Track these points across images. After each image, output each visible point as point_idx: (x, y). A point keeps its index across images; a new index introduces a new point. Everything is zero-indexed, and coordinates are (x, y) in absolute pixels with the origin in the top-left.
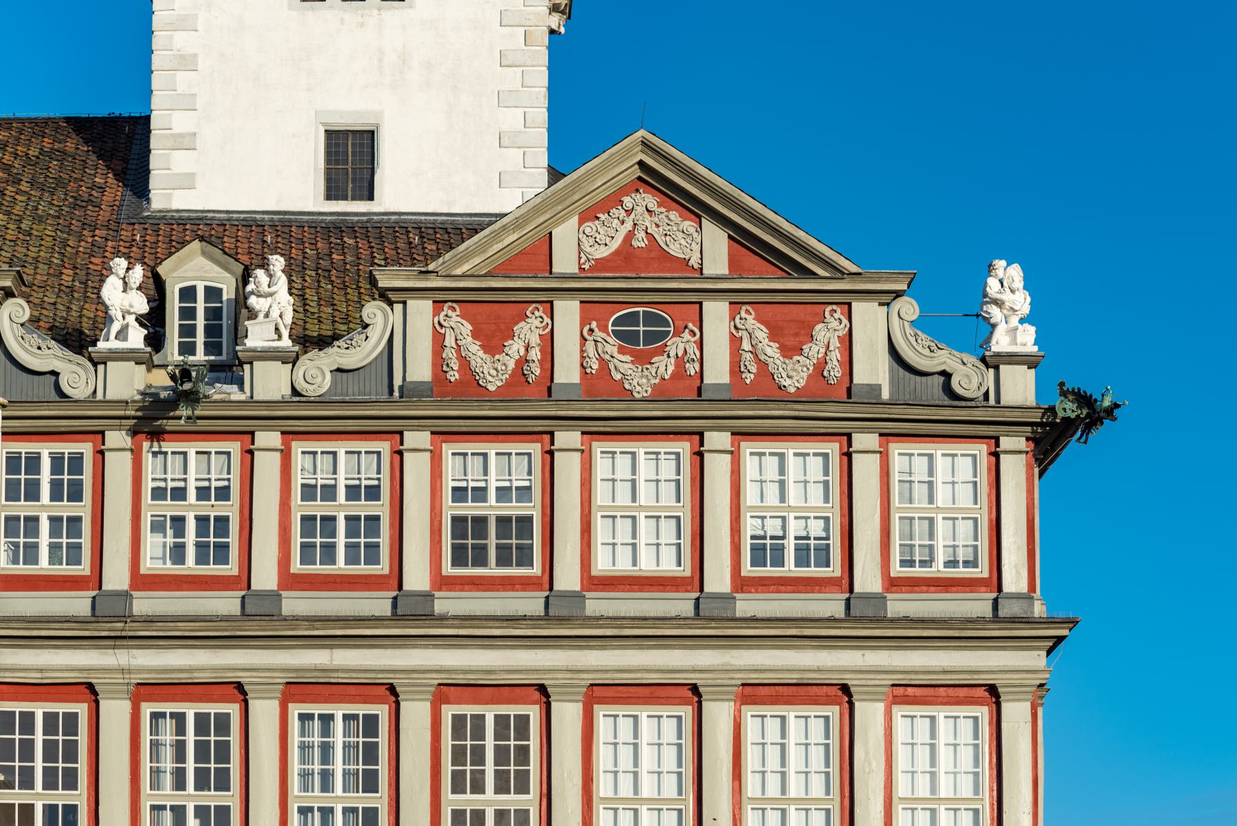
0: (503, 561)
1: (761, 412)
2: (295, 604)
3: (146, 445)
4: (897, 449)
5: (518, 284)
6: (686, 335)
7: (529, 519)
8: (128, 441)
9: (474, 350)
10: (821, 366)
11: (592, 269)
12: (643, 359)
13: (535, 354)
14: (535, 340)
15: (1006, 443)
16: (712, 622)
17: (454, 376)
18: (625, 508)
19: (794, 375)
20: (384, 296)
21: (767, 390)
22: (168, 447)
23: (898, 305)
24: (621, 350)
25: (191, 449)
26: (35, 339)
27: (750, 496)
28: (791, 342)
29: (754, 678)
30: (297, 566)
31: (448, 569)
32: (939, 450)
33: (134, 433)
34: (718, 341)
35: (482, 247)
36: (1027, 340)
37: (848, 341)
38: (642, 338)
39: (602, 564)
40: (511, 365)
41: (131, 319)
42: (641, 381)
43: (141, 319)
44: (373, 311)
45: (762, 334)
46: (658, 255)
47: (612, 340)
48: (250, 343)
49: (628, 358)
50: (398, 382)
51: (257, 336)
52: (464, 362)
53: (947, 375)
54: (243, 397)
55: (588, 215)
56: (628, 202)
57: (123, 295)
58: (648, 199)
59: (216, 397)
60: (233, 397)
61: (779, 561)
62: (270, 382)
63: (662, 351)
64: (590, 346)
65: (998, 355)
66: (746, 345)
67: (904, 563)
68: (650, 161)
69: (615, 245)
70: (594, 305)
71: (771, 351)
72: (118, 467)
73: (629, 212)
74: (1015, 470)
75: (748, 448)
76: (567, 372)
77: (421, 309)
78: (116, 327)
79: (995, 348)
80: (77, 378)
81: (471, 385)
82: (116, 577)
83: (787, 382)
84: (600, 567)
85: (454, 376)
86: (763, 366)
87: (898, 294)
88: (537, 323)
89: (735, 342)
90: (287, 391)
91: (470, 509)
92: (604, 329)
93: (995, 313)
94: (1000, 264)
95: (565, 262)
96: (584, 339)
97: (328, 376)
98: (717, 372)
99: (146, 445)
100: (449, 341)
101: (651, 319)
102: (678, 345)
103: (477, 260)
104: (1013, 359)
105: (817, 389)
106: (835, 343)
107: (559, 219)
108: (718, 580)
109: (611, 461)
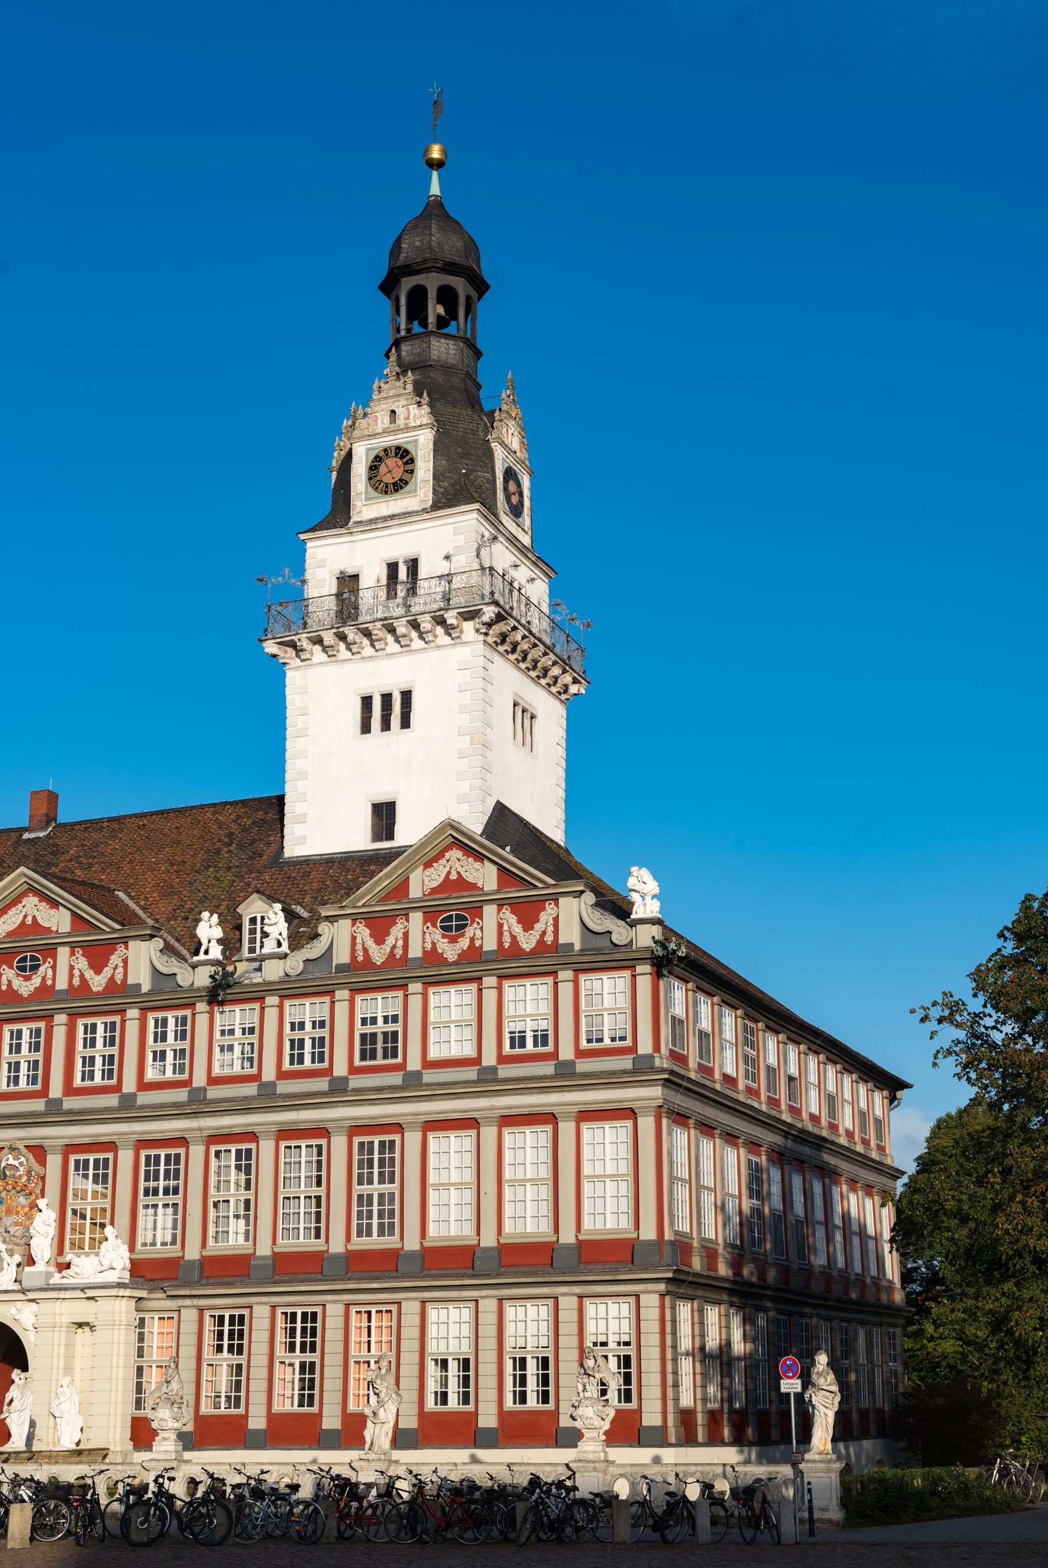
0: (385, 1057)
1: (513, 963)
2: (284, 1087)
3: (216, 1008)
4: (582, 977)
5: (388, 908)
6: (475, 925)
7: (397, 1032)
8: (207, 1008)
11: (429, 894)
12: (453, 940)
13: (400, 943)
14: (400, 935)
15: (640, 969)
16: (488, 1081)
17: (360, 959)
18: (449, 1023)
19: (528, 942)
20: (329, 919)
21: (515, 951)
22: (227, 1008)
23: (583, 896)
24: (444, 936)
25: (237, 1008)
26: (165, 958)
27: (509, 1010)
29: (506, 1112)
30: (286, 1065)
31: (357, 1062)
32: (605, 976)
33: (210, 1003)
35: (370, 890)
37: (556, 920)
38: (453, 928)
39: (434, 1054)
40: (388, 950)
41: (214, 942)
42: (450, 952)
43: (220, 941)
45: (513, 919)
46: (461, 884)
49: (446, 940)
51: (270, 947)
52: (365, 950)
54: (260, 980)
55: (428, 865)
56: (447, 855)
57: (209, 929)
58: (455, 854)
59: (246, 982)
60: (254, 981)
61: (523, 1044)
62: (273, 971)
63: (462, 935)
64: (427, 936)
65: (634, 920)
66: (505, 928)
67: (589, 1041)
72: (202, 1020)
73: (448, 861)
74: (644, 984)
75: (506, 984)
77: (347, 923)
80: (185, 977)
82: (199, 1080)
83: (524, 946)
84: (432, 1055)
85: (360, 959)
87: (582, 892)
88: (401, 926)
89: (500, 926)
90: (282, 974)
91: (369, 1029)
92: (434, 925)
95: (415, 891)
96: (424, 933)
97: (301, 965)
99: (216, 1008)
100: (359, 941)
101: (460, 917)
102: (469, 932)
103: (369, 897)
108: (489, 1059)
109: (437, 997)
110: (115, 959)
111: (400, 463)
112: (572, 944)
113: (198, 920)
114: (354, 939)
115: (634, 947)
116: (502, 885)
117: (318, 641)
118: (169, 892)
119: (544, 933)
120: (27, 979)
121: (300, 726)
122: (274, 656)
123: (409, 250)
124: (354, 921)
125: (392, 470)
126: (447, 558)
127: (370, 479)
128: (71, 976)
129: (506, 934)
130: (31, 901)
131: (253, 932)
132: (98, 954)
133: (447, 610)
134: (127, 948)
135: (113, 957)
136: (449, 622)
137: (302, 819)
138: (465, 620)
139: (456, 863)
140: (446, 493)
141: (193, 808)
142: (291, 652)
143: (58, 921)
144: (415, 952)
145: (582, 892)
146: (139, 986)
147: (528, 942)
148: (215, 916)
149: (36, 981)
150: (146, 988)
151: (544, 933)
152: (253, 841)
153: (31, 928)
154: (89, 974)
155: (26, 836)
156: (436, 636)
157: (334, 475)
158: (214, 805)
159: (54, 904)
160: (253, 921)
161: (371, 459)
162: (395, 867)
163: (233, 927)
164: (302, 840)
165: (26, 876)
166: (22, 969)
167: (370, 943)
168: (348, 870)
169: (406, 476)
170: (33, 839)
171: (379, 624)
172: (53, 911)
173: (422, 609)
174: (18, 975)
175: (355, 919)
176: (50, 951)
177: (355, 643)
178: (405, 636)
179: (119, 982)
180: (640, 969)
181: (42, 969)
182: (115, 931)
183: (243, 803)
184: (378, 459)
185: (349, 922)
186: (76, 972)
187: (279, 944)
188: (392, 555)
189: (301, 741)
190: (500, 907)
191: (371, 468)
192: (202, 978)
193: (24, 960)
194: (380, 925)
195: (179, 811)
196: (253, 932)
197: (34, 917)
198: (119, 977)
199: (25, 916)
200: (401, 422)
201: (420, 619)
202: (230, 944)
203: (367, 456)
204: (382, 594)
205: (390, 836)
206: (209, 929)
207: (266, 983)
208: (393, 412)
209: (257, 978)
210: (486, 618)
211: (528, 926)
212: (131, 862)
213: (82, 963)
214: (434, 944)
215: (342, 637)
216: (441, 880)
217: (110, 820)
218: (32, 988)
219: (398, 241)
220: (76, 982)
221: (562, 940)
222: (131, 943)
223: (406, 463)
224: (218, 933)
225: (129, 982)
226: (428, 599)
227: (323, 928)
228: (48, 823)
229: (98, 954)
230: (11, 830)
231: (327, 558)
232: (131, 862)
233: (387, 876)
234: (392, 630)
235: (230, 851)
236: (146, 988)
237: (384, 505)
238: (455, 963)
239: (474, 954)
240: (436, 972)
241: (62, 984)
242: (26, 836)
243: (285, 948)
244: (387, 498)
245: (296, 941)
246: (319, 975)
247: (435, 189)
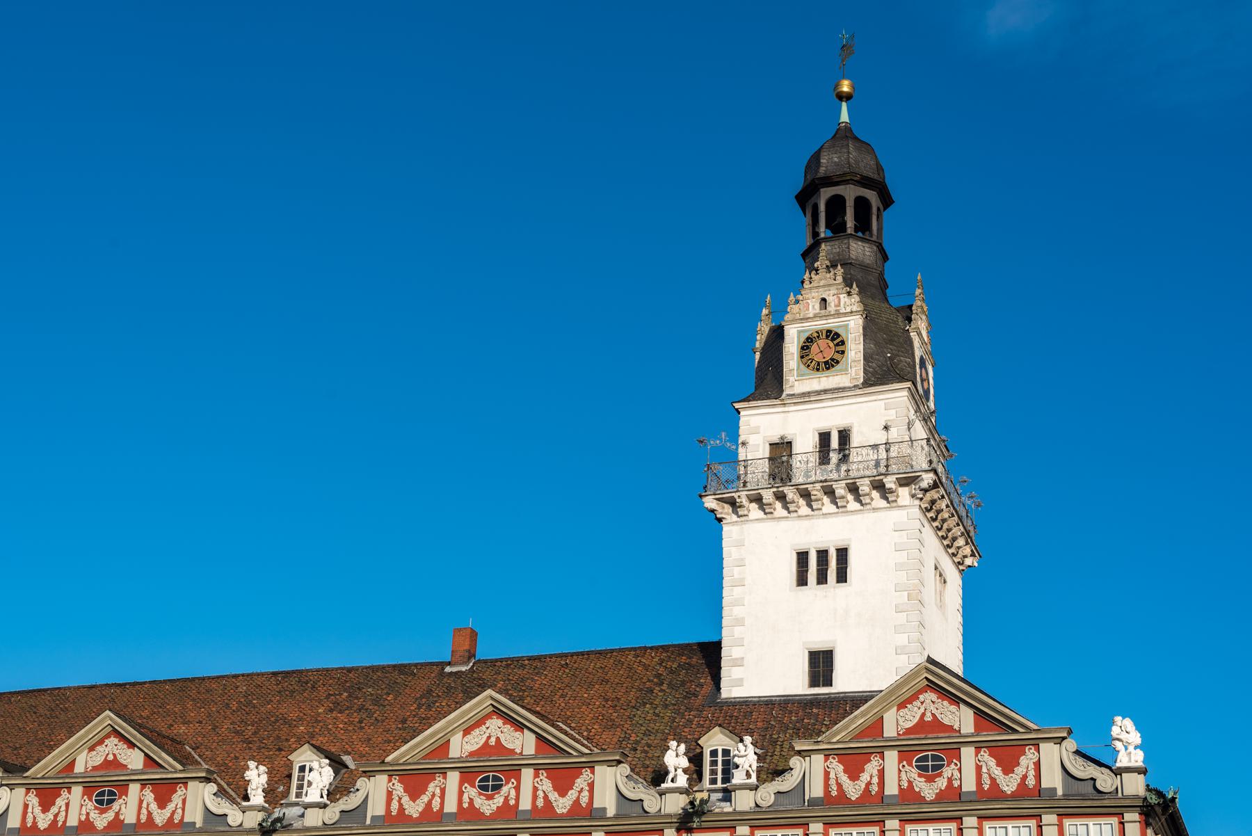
12: (930, 780)
13: (875, 780)
14: (875, 772)
15: (1128, 817)
17: (834, 793)
19: (1009, 784)
20: (799, 753)
21: (995, 793)
23: (1065, 743)
24: (920, 775)
26: (632, 784)
32: (1091, 822)
34: (969, 770)
35: (846, 727)
36: (1138, 759)
37: (1038, 765)
38: (930, 769)
40: (863, 786)
41: (680, 771)
42: (928, 791)
43: (685, 771)
44: (795, 762)
45: (992, 762)
46: (936, 725)
47: (915, 770)
48: (734, 781)
50: (807, 798)
51: (738, 778)
53: (1094, 780)
54: (730, 810)
55: (902, 706)
57: (675, 759)
58: (930, 696)
60: (726, 810)
62: (744, 801)
63: (940, 775)
64: (903, 775)
65: (1119, 768)
66: (984, 770)
68: (930, 677)
69: (916, 720)
76: (891, 789)
77: (818, 759)
78: (670, 776)
79: (1118, 765)
80: (652, 803)
81: (842, 797)
83: (1005, 789)
85: (834, 793)
87: (1064, 738)
89: (979, 768)
92: (910, 764)
93: (1119, 745)
94: (1118, 719)
95: (890, 731)
98: (969, 785)
100: (832, 775)
101: (935, 758)
102: (947, 772)
104: (1128, 770)
105: (1023, 791)
106: (1032, 766)
107: (886, 709)
110: (581, 782)
111: (831, 344)
112: (1055, 789)
113: (668, 748)
114: (827, 774)
115: (1120, 795)
116: (978, 728)
117: (758, 500)
118: (611, 725)
119: (1025, 777)
120: (490, 798)
121: (736, 576)
122: (713, 511)
123: (830, 162)
124: (827, 757)
125: (824, 351)
126: (886, 428)
127: (802, 357)
128: (535, 797)
129: (985, 776)
130: (495, 723)
131: (714, 763)
132: (563, 777)
133: (886, 475)
134: (593, 773)
135: (578, 781)
136: (887, 486)
137: (739, 662)
138: (901, 485)
139: (931, 705)
140: (874, 373)
141: (612, 651)
142: (728, 508)
143: (524, 743)
144: (891, 789)
145: (1064, 738)
146: (604, 809)
147: (1009, 784)
148: (683, 746)
149: (499, 800)
150: (611, 812)
151: (1025, 777)
152: (683, 683)
153: (494, 749)
154: (553, 796)
155: (448, 669)
156: (872, 499)
157: (758, 356)
158: (634, 649)
159: (519, 726)
160: (714, 753)
161: (803, 339)
162: (872, 707)
163: (696, 759)
164: (739, 682)
165: (492, 698)
166: (484, 788)
167: (844, 779)
168: (791, 712)
169: (837, 356)
170: (456, 673)
171: (818, 486)
172: (518, 734)
173: (862, 473)
174: (480, 794)
176: (514, 772)
177: (793, 502)
178: (843, 497)
179: (584, 805)
180: (1128, 817)
181: (505, 790)
182: (583, 754)
183: (664, 648)
184: (810, 340)
185: (821, 757)
186: (540, 794)
187: (748, 775)
189: (737, 591)
190: (978, 750)
191: (802, 348)
192: (675, 804)
193: (486, 779)
194: (854, 762)
195: (600, 653)
196: (714, 763)
197: (498, 739)
198: (584, 800)
199: (489, 737)
200: (831, 308)
201: (859, 482)
202: (695, 771)
203: (799, 338)
204: (814, 459)
205: (829, 683)
206: (675, 759)
207: (735, 812)
208: (824, 300)
209: (727, 808)
210: (924, 485)
211: (1008, 770)
212: (562, 696)
213: (546, 785)
214: (910, 783)
215: (781, 497)
217: (530, 658)
218: (494, 807)
219: (816, 158)
220: (540, 803)
222: (597, 768)
223: (837, 345)
224: (684, 762)
225: (595, 806)
226: (861, 466)
227: (795, 762)
228: (469, 658)
229: (563, 777)
230: (432, 664)
231: (759, 425)
232: (562, 696)
233: (863, 714)
234: (830, 492)
235: (662, 690)
236: (611, 812)
237: (815, 381)
238: (931, 803)
241: (525, 804)
242: (448, 669)
243: (754, 780)
244: (818, 374)
246: (790, 807)
247: (845, 117)
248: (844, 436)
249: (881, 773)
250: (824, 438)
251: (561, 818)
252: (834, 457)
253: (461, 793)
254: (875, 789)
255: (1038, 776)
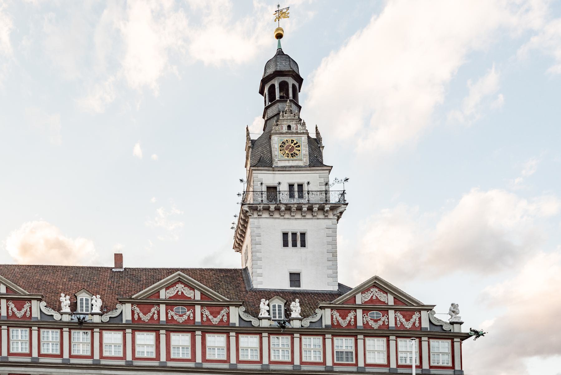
9: (339, 319)
10: (414, 323)
13: (353, 320)
20: (321, 308)
28: (408, 318)
44: (317, 311)
52: (338, 322)
70: (366, 310)
71: (403, 320)
85: (335, 324)
86: (402, 323)
100: (334, 317)
114: (332, 316)
120: (180, 316)
124: (332, 310)
128: (202, 317)
149: (185, 317)
175: (332, 309)
185: (330, 310)
188: (291, 181)
194: (344, 311)
213: (207, 313)
216: (369, 298)
221: (423, 326)
227: (317, 311)
239: (386, 326)
240: (369, 333)
245: (304, 315)
248: (300, 186)
249: (355, 317)
250: (291, 186)
251: (214, 326)
252: (296, 194)
253: (167, 314)
254: (352, 323)
255: (420, 323)
